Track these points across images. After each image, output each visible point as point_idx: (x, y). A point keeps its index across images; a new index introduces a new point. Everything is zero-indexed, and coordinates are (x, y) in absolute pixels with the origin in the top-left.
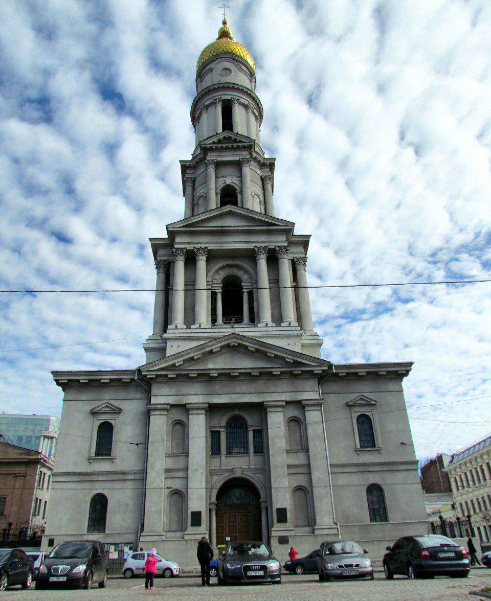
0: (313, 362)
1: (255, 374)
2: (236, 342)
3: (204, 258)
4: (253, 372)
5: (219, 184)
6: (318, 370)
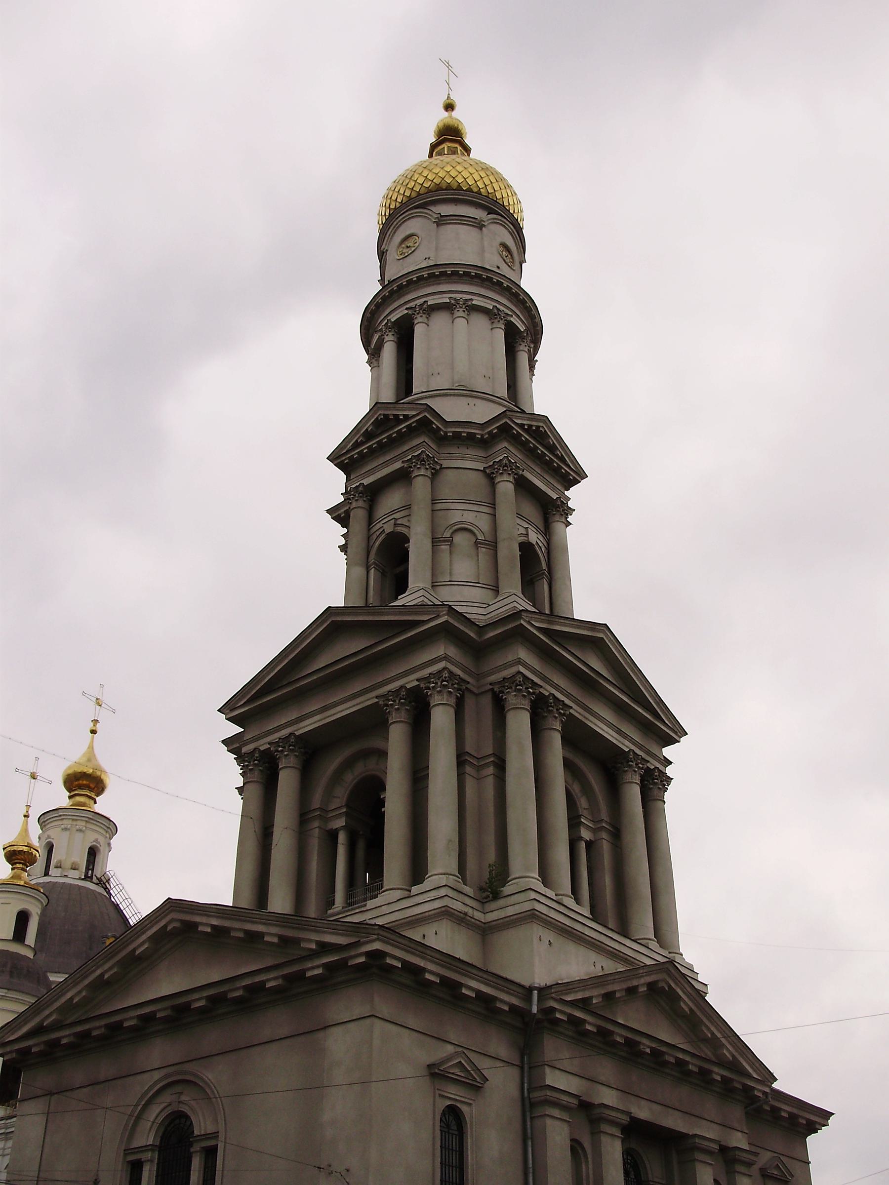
3: (292, 761)
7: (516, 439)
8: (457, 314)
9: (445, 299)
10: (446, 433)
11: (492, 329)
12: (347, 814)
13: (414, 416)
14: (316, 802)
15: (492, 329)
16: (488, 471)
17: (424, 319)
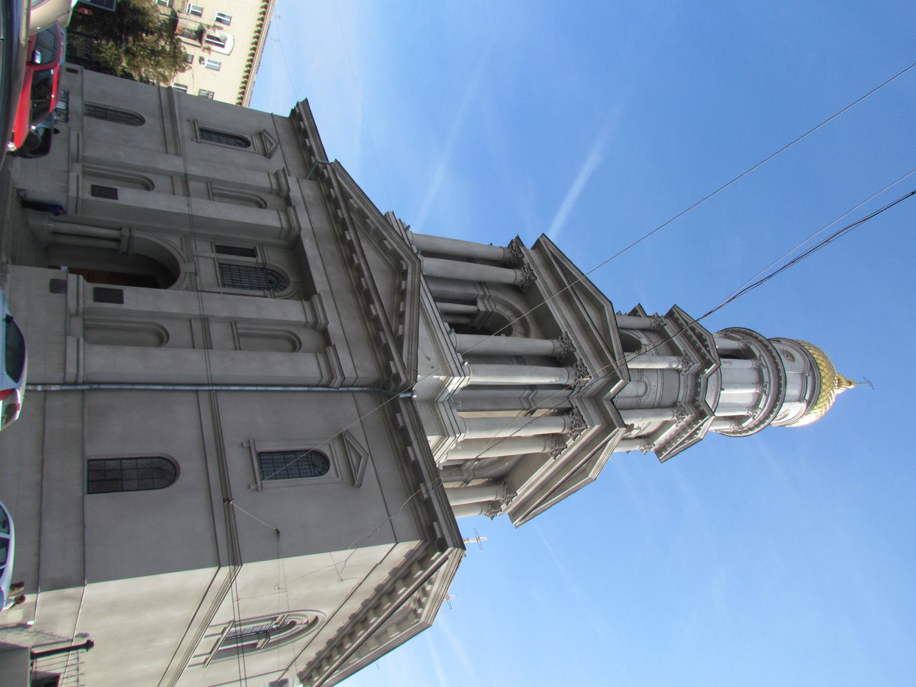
0: (408, 359)
1: (364, 283)
2: (407, 267)
4: (365, 280)
5: (636, 333)
6: (395, 366)
8: (758, 385)
9: (766, 379)
10: (700, 378)
11: (747, 407)
12: (487, 312)
14: (493, 293)
16: (678, 404)
17: (755, 366)
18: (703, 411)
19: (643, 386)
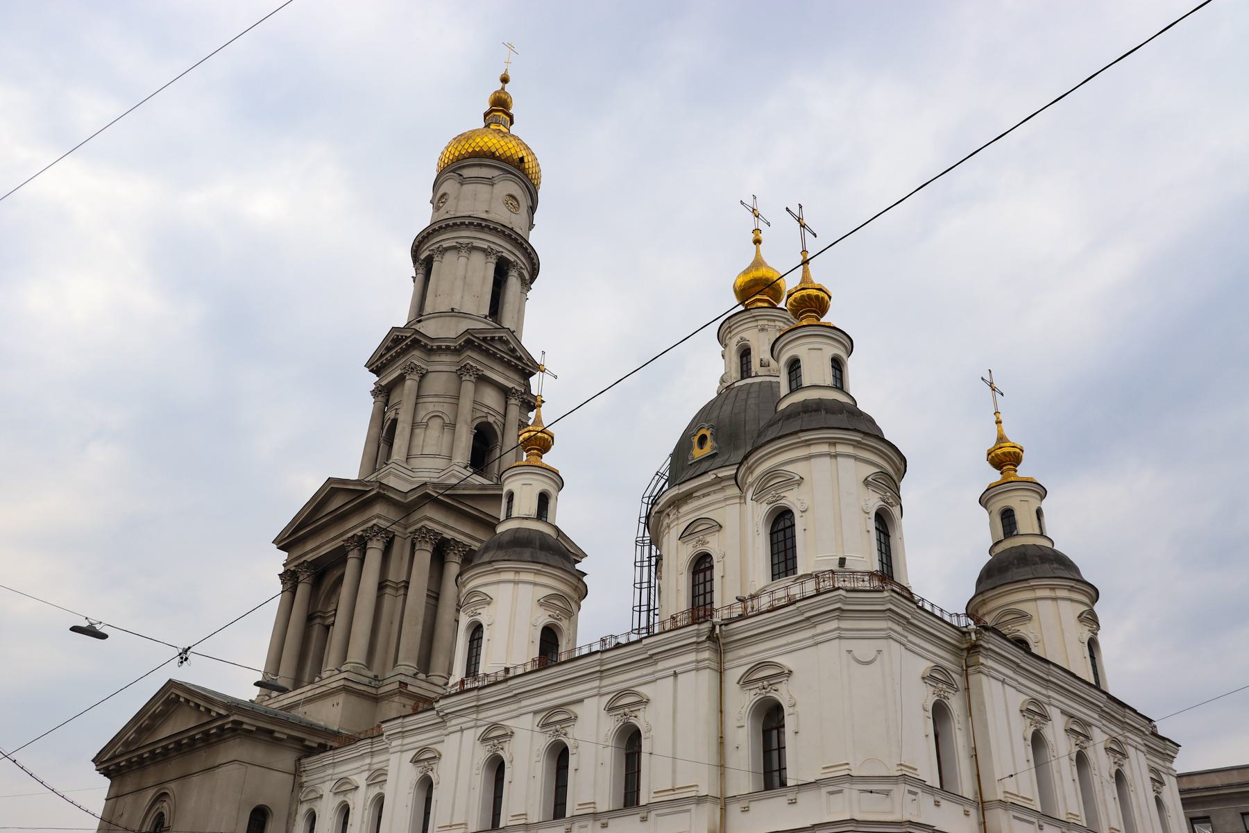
7: (479, 349)
8: (461, 253)
10: (432, 347)
11: (486, 263)
13: (410, 337)
15: (486, 263)
18: (464, 341)
19: (433, 419)
